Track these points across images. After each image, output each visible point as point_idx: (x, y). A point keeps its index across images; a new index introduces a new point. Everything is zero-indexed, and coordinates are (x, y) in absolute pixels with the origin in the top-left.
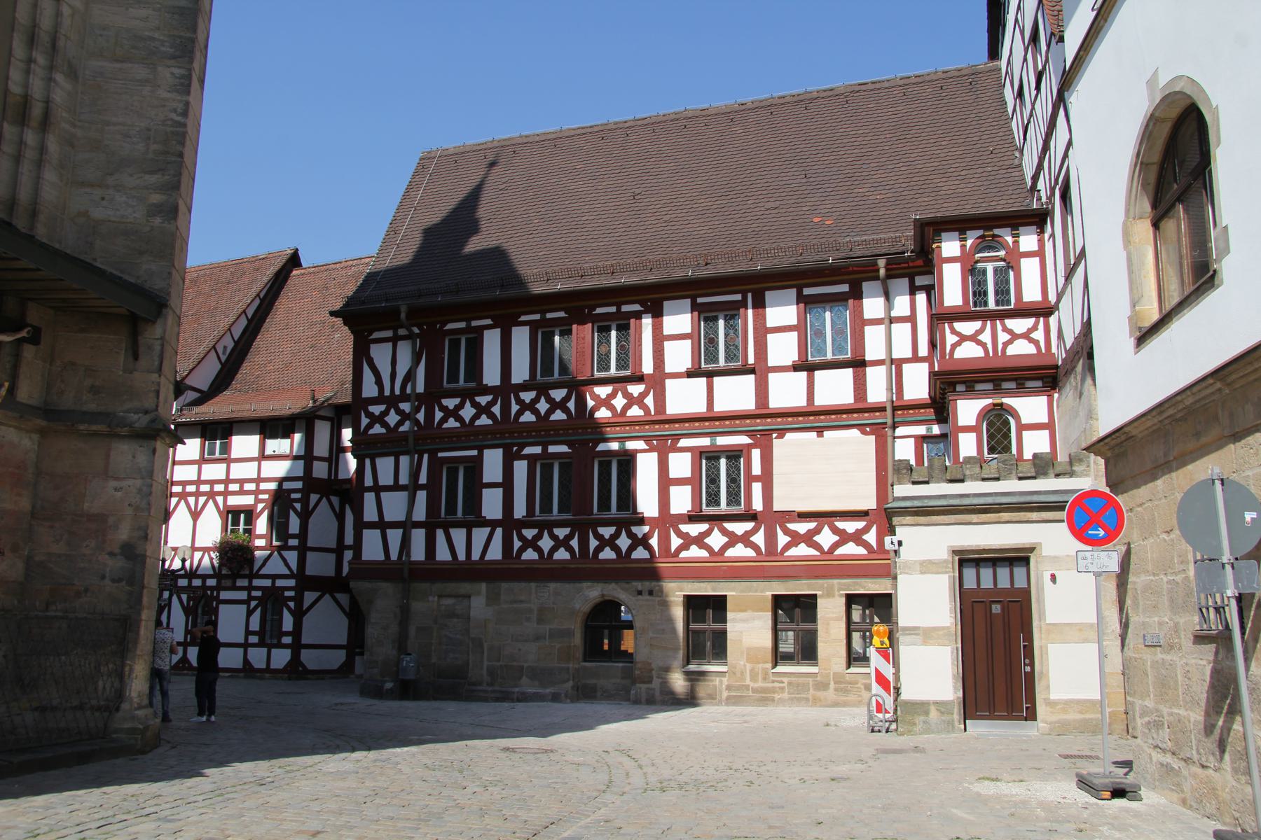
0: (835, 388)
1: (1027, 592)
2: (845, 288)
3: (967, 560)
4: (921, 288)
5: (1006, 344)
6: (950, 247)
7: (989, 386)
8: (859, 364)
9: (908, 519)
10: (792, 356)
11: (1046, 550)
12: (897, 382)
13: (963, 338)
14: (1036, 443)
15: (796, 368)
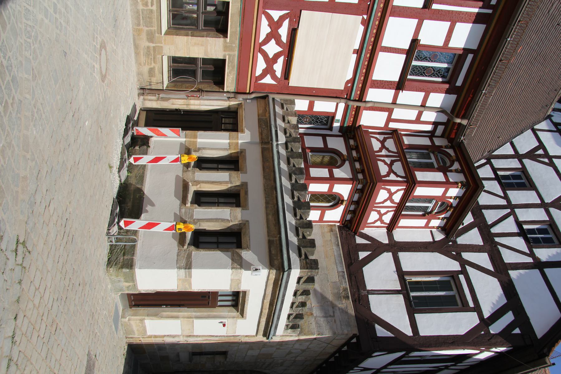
0: (388, 67)
2: (459, 83)
7: (356, 198)
9: (273, 276)
10: (424, 39)
11: (240, 321)
12: (377, 107)
13: (391, 194)
15: (415, 42)
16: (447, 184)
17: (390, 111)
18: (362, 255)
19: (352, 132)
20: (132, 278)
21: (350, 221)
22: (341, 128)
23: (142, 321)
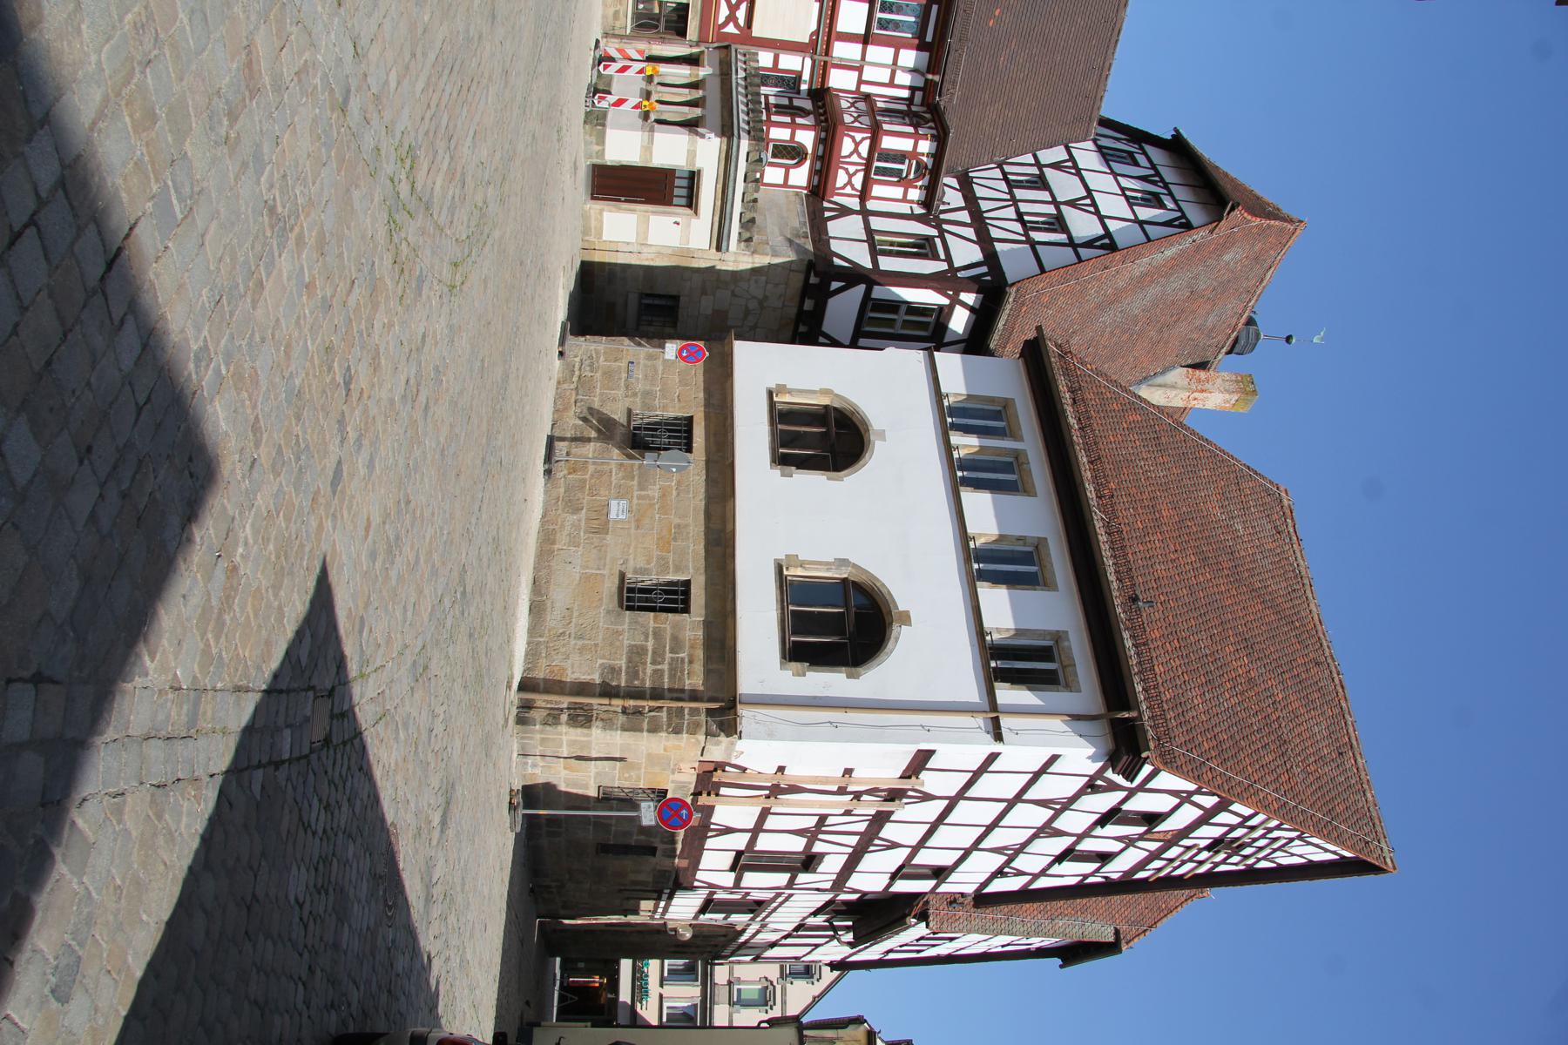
1: (669, 203)
2: (929, 38)
3: (693, 178)
4: (913, 95)
5: (847, 170)
6: (925, 146)
7: (820, 153)
8: (866, 39)
9: (724, 147)
11: (694, 221)
13: (857, 145)
14: (773, 175)
16: (916, 137)
17: (860, 70)
18: (827, 214)
19: (821, 95)
20: (601, 140)
21: (818, 186)
22: (810, 90)
23: (601, 211)
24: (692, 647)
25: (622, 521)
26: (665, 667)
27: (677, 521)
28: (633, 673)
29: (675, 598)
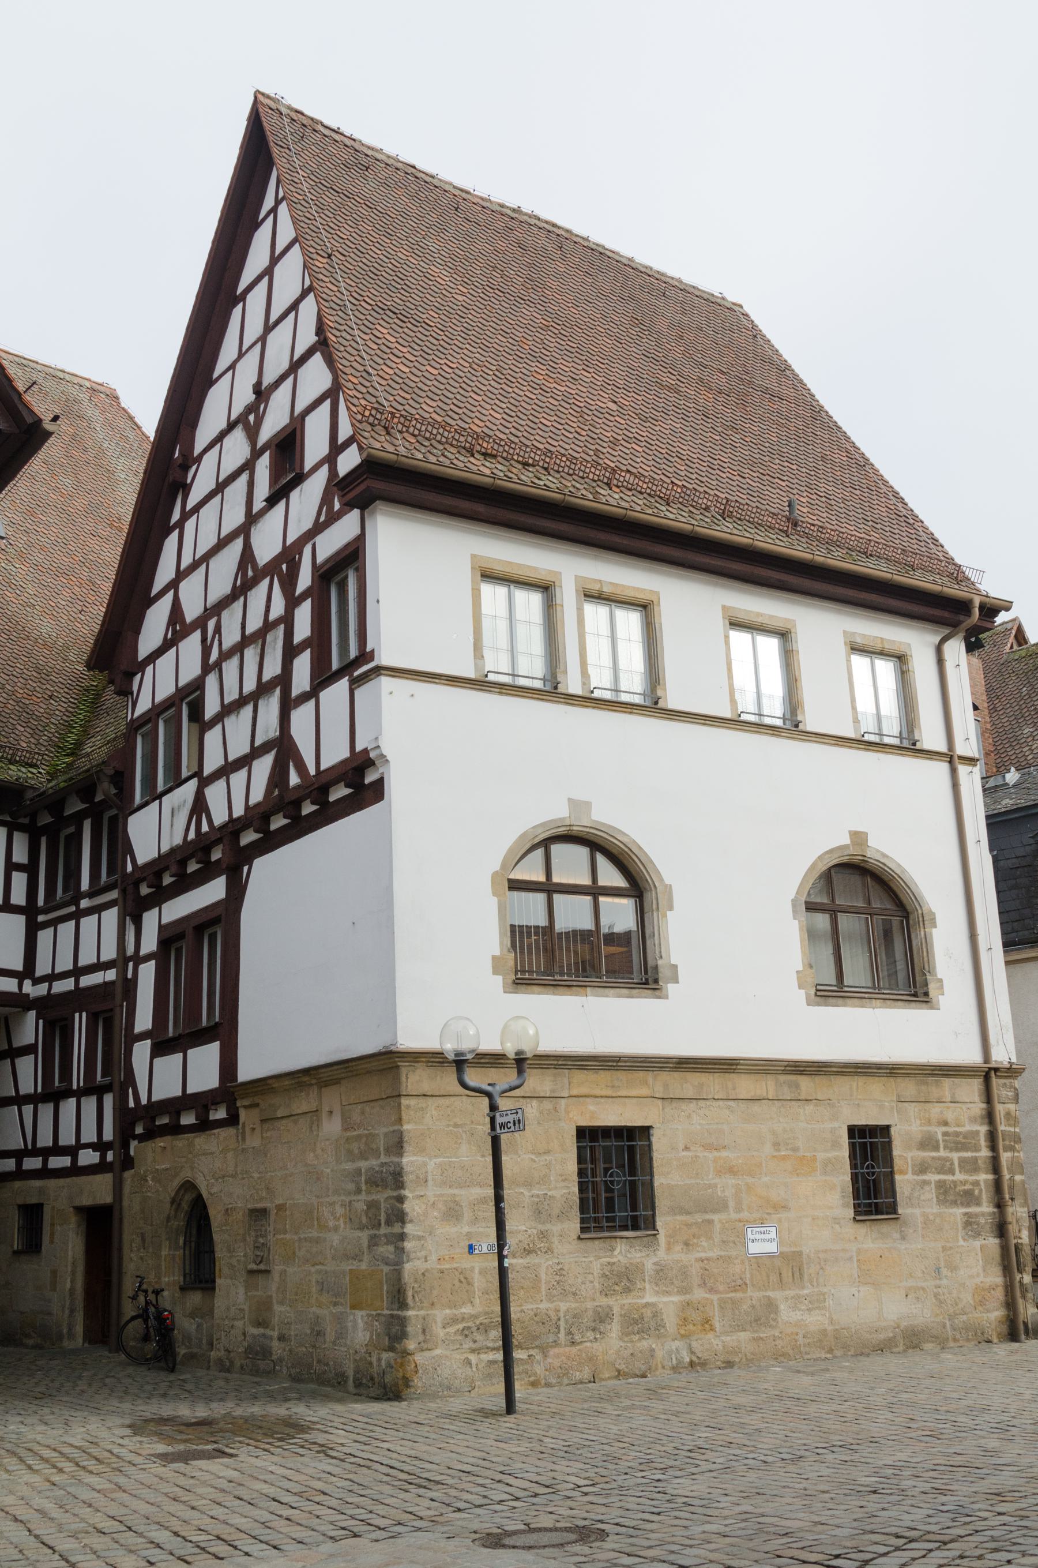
24: (929, 1122)
25: (779, 1233)
26: (955, 1156)
27: (768, 1149)
28: (969, 1197)
29: (869, 1146)
